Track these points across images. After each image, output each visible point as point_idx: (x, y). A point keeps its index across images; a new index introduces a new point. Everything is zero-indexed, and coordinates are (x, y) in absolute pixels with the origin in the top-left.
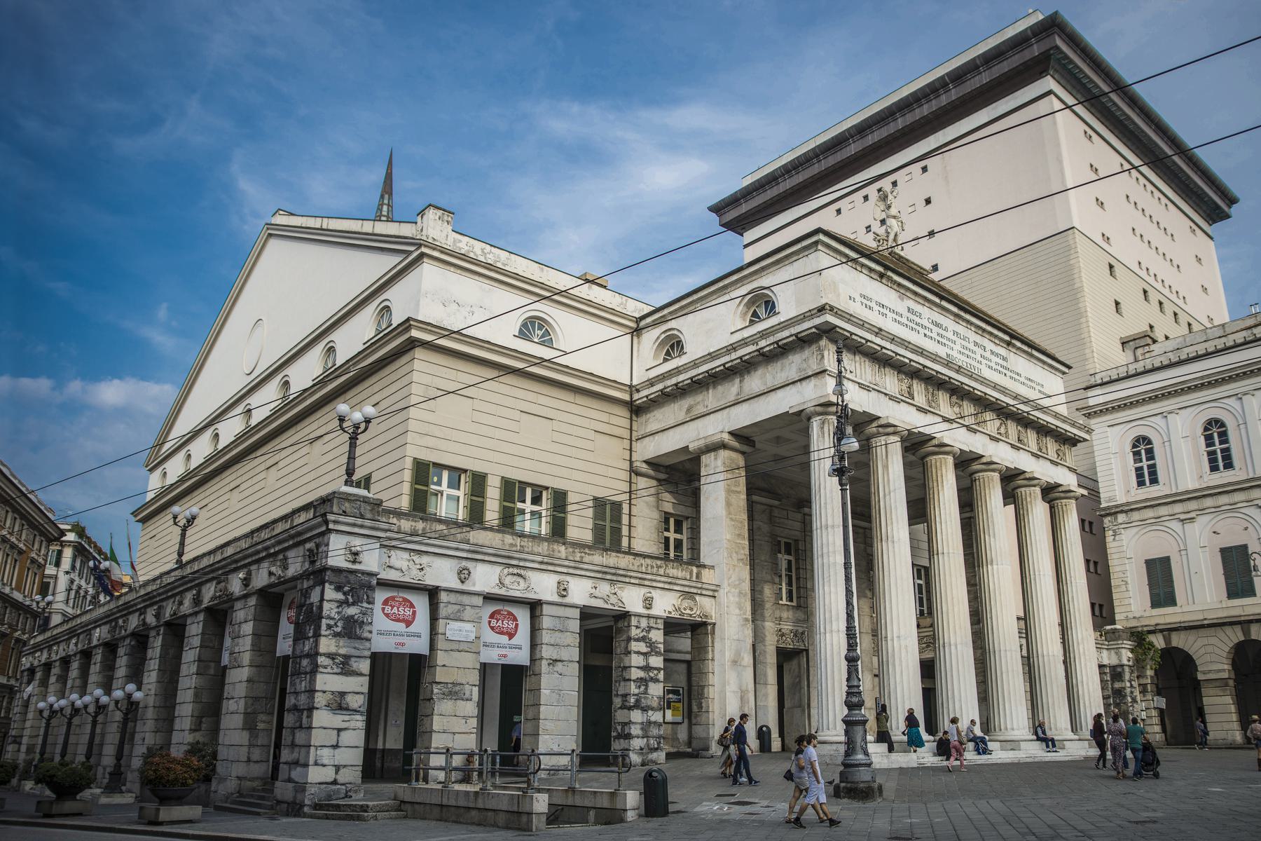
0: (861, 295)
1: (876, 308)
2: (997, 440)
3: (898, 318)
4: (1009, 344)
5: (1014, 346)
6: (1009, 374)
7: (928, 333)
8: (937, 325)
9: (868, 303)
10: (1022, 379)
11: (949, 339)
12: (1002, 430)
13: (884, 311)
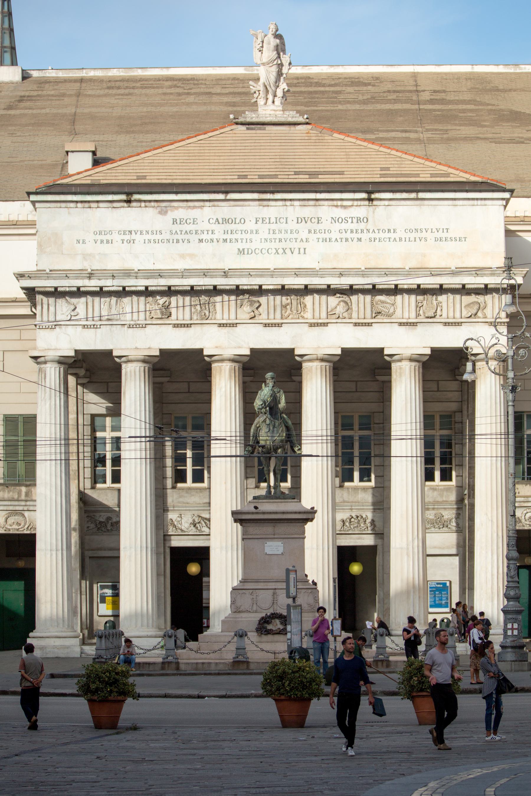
0: (95, 233)
1: (117, 237)
2: (325, 324)
4: (370, 200)
5: (381, 200)
6: (365, 236)
7: (204, 237)
8: (226, 221)
9: (104, 238)
10: (400, 234)
11: (246, 232)
12: (341, 309)
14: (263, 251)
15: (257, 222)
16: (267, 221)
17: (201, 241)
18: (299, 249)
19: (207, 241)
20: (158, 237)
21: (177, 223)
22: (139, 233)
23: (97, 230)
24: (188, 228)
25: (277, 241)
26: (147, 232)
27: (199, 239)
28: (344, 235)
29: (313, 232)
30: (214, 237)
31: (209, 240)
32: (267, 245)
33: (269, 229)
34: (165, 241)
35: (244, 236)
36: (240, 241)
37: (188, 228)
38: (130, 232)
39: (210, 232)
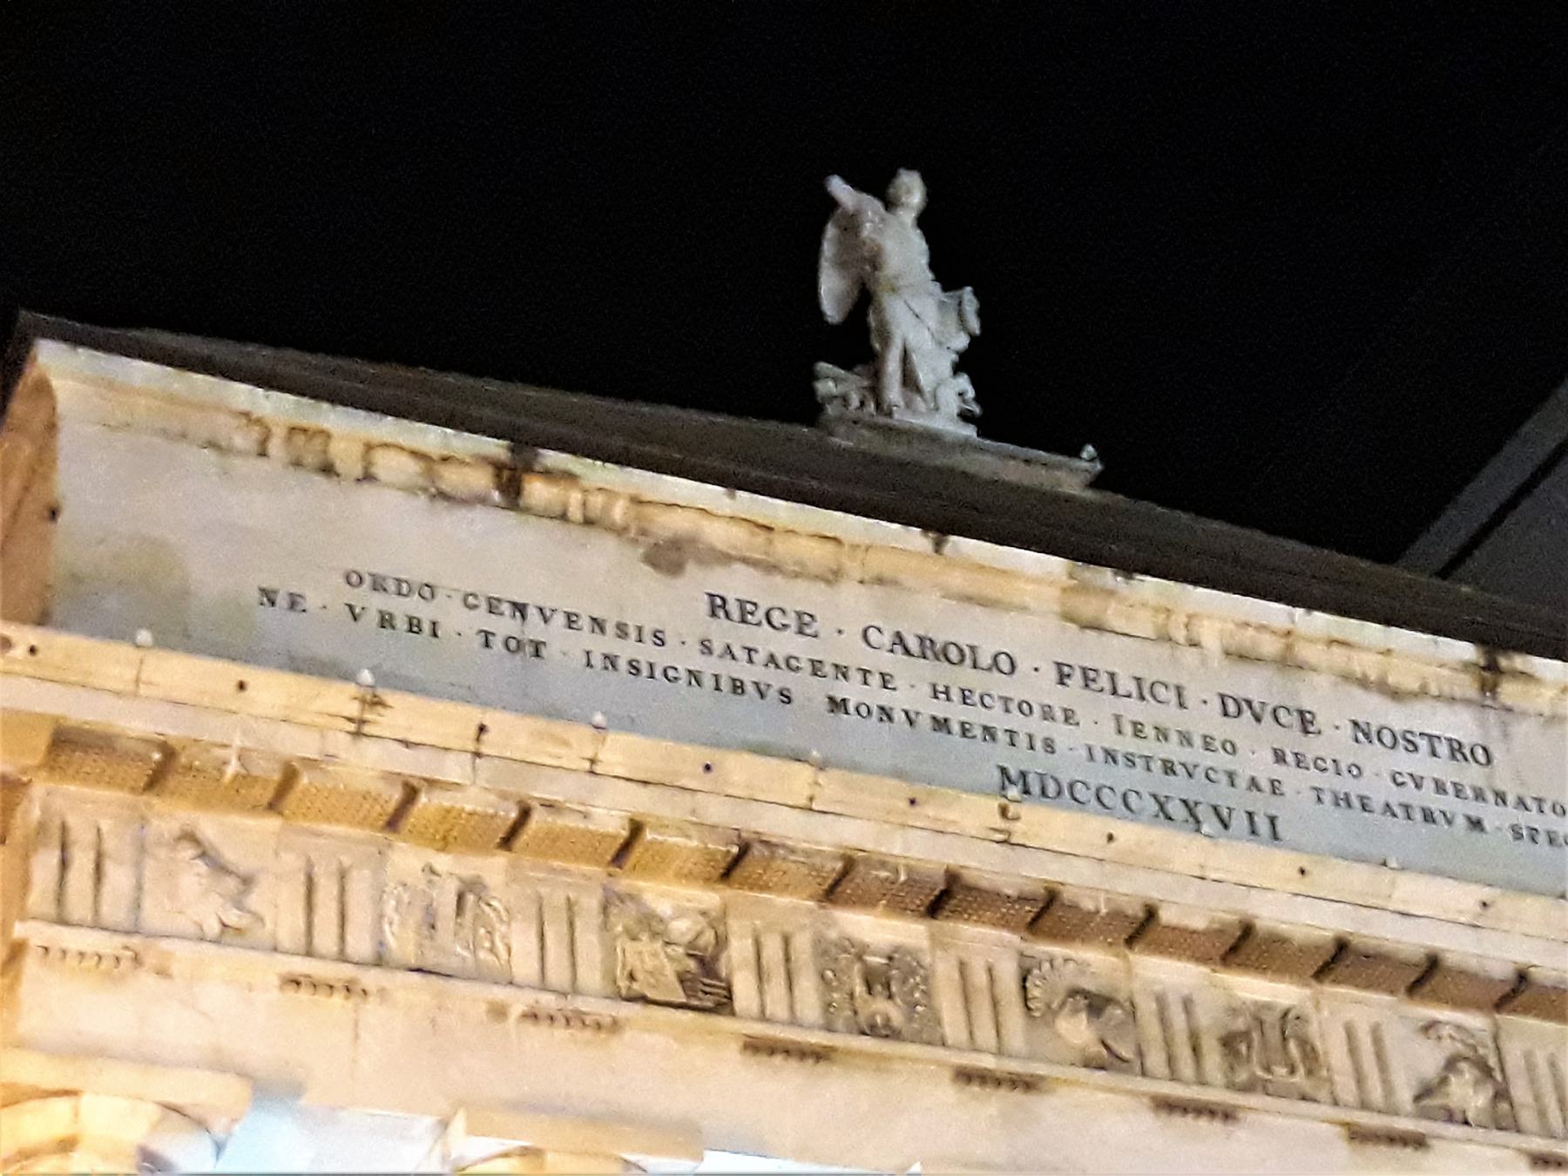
0: (353, 579)
3: (626, 650)
6: (1490, 813)
7: (851, 691)
8: (931, 650)
13: (534, 629)
14: (1106, 795)
15: (1062, 679)
16: (1104, 681)
17: (838, 705)
18: (1250, 815)
19: (864, 711)
20: (646, 653)
21: (727, 615)
22: (559, 620)
23: (364, 569)
24: (786, 644)
25: (1157, 766)
26: (598, 624)
27: (831, 699)
28: (1409, 794)
29: (1290, 758)
30: (898, 701)
31: (875, 710)
32: (1122, 777)
33: (1118, 718)
34: (683, 675)
35: (1015, 721)
36: (1003, 737)
37: (786, 644)
38: (520, 609)
39: (875, 680)
